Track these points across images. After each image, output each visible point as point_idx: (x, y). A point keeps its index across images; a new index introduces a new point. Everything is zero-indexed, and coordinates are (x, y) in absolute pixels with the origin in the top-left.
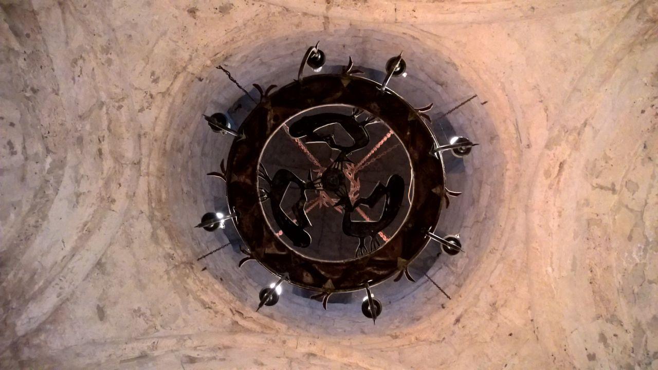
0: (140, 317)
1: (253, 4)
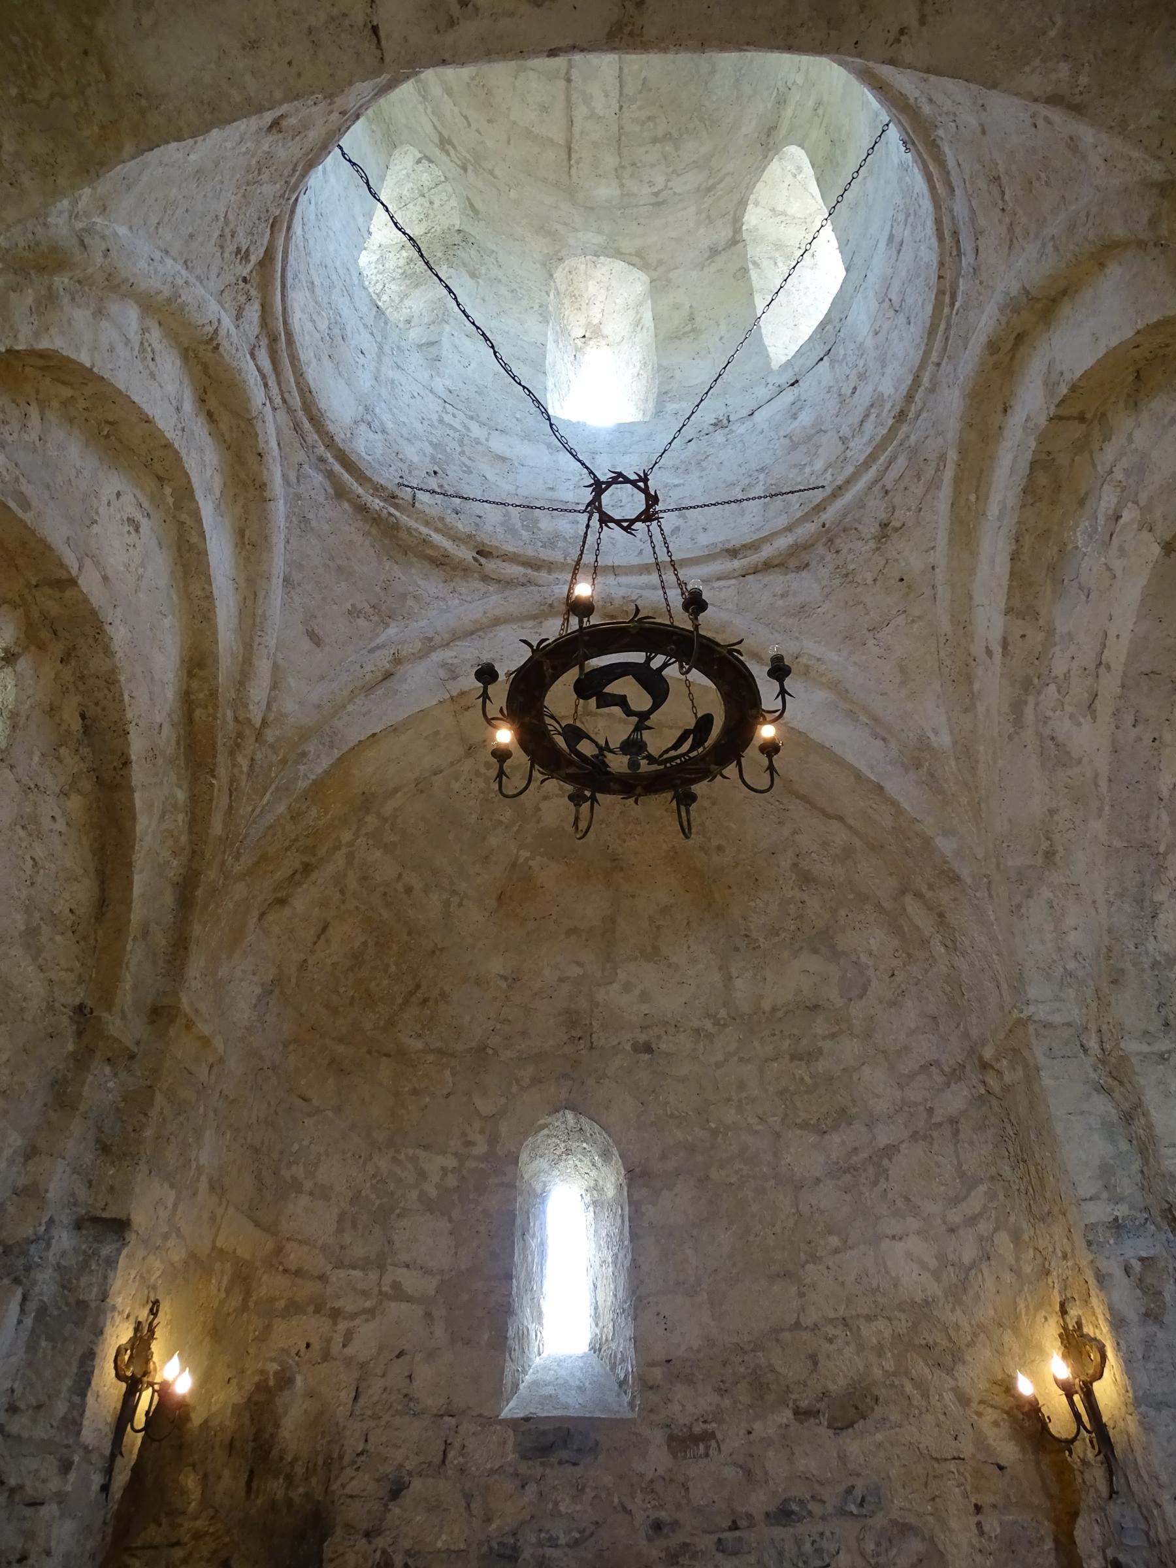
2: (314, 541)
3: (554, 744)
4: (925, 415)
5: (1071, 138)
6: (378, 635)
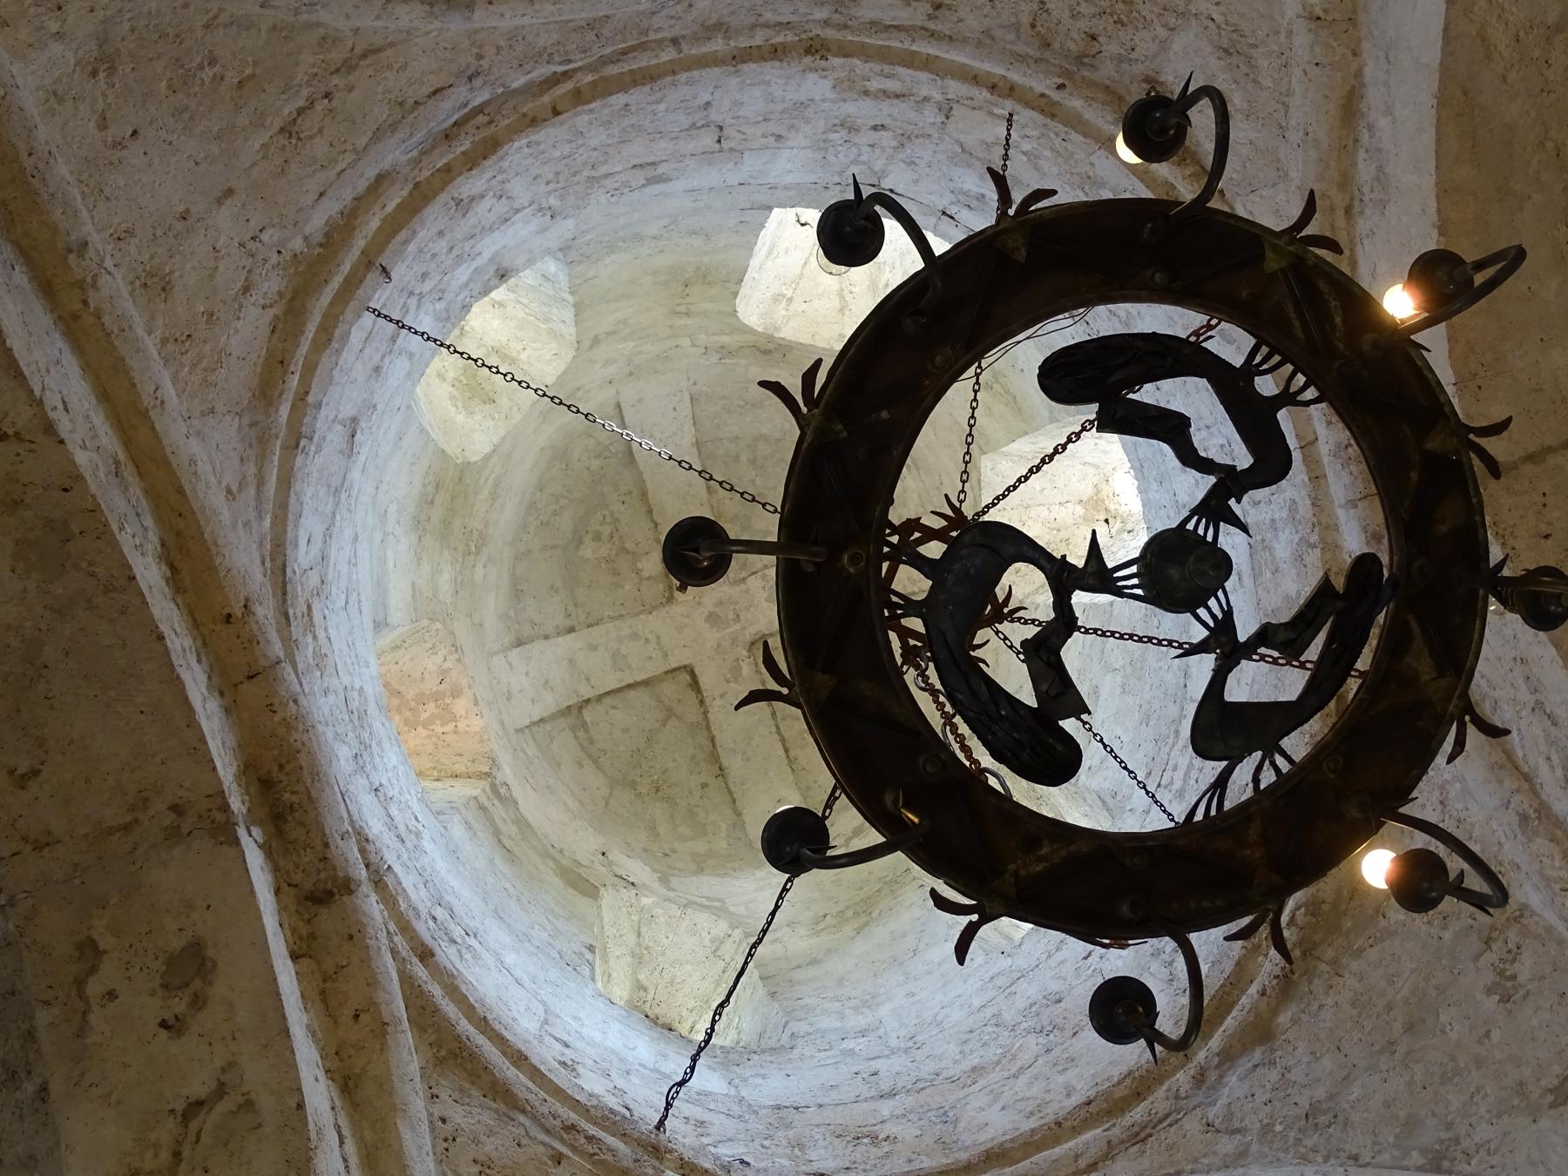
0: (1514, 977)
1: (444, 1121)
2: (1356, 1092)
3: (1321, 752)
4: (769, 16)
5: (94, 74)
6: (1549, 929)
